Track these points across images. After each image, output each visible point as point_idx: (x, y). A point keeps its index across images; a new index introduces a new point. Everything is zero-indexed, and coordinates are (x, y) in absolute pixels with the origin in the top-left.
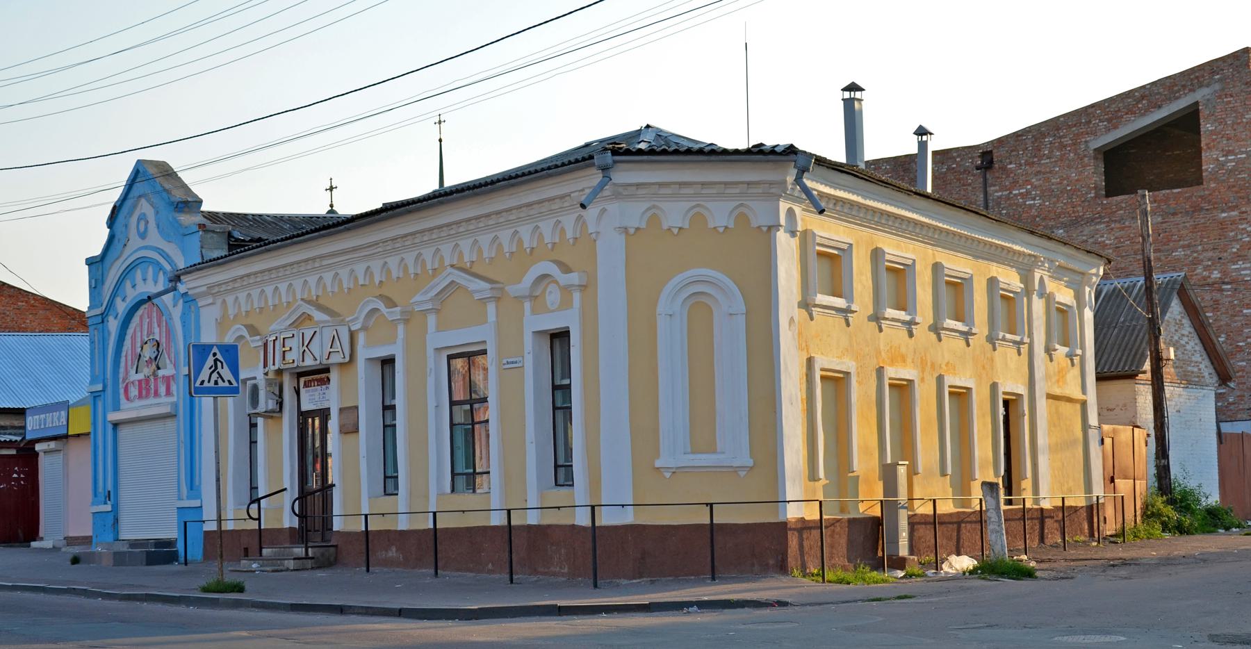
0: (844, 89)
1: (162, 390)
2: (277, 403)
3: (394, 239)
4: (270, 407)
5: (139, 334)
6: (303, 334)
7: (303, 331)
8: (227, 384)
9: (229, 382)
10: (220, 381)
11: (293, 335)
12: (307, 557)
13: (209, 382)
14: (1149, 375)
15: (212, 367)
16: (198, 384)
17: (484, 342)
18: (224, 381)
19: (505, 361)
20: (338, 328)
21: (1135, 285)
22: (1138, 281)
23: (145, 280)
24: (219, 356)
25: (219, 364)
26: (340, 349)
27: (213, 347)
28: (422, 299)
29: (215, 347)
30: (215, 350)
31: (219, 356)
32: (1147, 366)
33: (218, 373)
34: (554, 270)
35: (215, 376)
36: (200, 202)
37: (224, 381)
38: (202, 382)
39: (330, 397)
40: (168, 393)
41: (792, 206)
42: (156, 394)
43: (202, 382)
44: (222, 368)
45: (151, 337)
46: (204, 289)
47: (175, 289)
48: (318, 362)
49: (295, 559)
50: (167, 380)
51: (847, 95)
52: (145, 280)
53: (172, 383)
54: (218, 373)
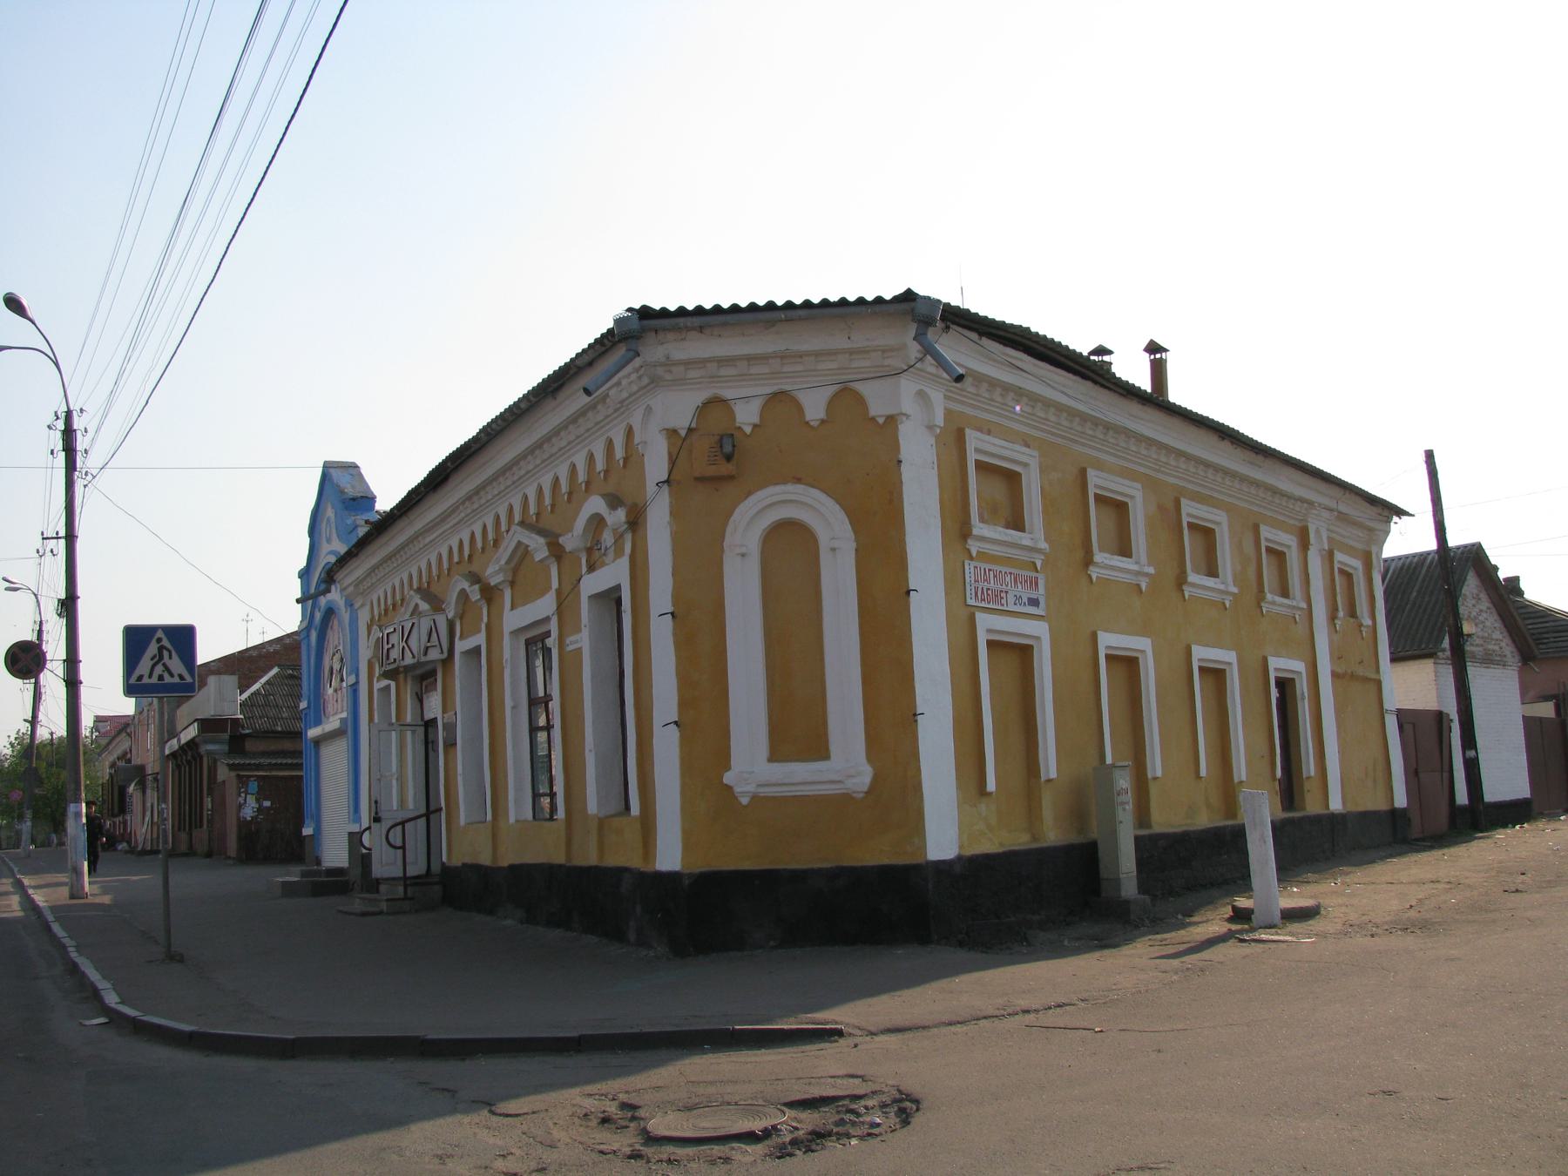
7: (402, 624)
8: (176, 680)
9: (181, 677)
10: (166, 675)
11: (395, 629)
12: (405, 898)
13: (150, 676)
14: (1448, 653)
15: (155, 656)
16: (133, 680)
18: (172, 675)
20: (434, 617)
25: (165, 653)
26: (437, 643)
31: (166, 642)
32: (1446, 643)
33: (164, 665)
35: (159, 669)
37: (172, 675)
38: (140, 678)
41: (922, 387)
43: (140, 678)
44: (170, 658)
48: (416, 660)
49: (388, 900)
54: (164, 665)
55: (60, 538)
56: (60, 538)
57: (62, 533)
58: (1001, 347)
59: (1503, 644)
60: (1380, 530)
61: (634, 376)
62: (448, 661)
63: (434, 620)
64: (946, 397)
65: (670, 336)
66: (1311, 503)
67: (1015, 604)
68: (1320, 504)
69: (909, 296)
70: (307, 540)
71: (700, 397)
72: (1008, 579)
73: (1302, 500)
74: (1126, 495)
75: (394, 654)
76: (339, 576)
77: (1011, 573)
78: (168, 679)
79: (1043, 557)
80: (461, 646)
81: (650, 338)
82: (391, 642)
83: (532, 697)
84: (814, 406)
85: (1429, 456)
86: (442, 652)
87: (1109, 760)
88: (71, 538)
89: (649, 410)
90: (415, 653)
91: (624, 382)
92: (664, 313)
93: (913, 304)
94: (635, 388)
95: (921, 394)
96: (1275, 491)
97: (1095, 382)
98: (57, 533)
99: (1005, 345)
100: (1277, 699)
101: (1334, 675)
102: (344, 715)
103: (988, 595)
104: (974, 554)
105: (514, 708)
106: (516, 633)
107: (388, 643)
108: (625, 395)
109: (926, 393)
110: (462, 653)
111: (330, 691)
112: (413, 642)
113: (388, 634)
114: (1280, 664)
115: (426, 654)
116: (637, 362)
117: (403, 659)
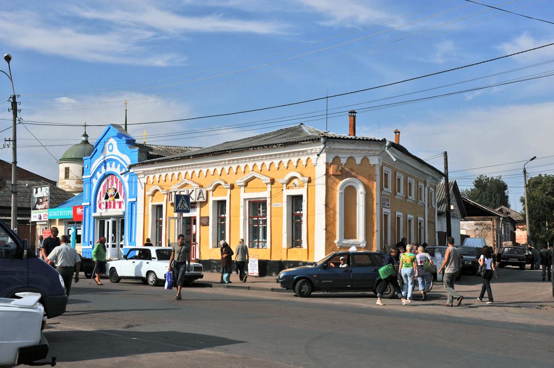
1: (117, 206)
3: (229, 161)
5: (106, 186)
8: (186, 209)
17: (266, 198)
19: (274, 204)
23: (111, 167)
28: (239, 181)
30: (183, 197)
34: (298, 175)
35: (182, 206)
36: (135, 141)
39: (195, 213)
40: (120, 207)
42: (114, 207)
45: (112, 187)
46: (141, 172)
47: (129, 171)
50: (120, 203)
52: (111, 167)
53: (122, 204)
62: (205, 203)
65: (331, 143)
71: (334, 156)
73: (428, 175)
78: (184, 209)
84: (358, 161)
85: (446, 153)
88: (15, 141)
96: (423, 173)
101: (428, 222)
115: (198, 199)
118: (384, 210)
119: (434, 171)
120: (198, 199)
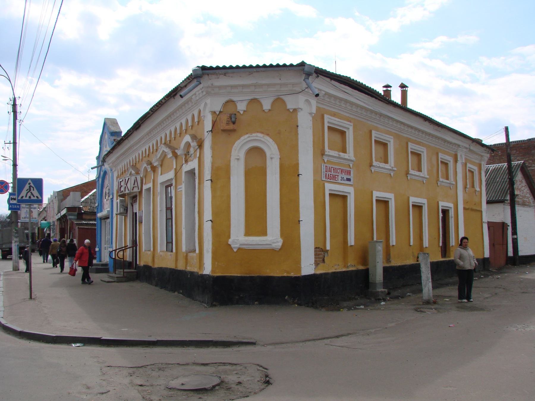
0: (384, 87)
2: (124, 210)
4: (121, 211)
6: (125, 179)
7: (125, 178)
8: (36, 198)
9: (37, 197)
11: (123, 180)
13: (26, 196)
14: (509, 201)
15: (28, 189)
18: (34, 196)
21: (503, 166)
22: (505, 165)
24: (32, 185)
25: (32, 188)
26: (137, 186)
27: (28, 181)
29: (30, 180)
31: (32, 185)
32: (508, 198)
33: (31, 193)
35: (29, 194)
37: (34, 196)
38: (22, 197)
41: (308, 99)
43: (22, 197)
44: (34, 190)
51: (385, 89)
54: (31, 193)
55: (11, 143)
56: (11, 143)
57: (12, 142)
58: (339, 84)
59: (530, 199)
60: (485, 156)
61: (200, 91)
62: (140, 192)
63: (136, 177)
64: (317, 102)
65: (214, 76)
66: (459, 146)
67: (341, 180)
68: (462, 146)
69: (302, 64)
70: (99, 146)
71: (224, 100)
72: (339, 171)
73: (455, 144)
74: (387, 141)
75: (122, 189)
76: (107, 160)
77: (340, 169)
78: (32, 198)
79: (353, 163)
80: (145, 187)
81: (206, 77)
82: (121, 185)
83: (167, 207)
84: (267, 105)
85: (507, 129)
86: (139, 189)
87: (375, 239)
88: (15, 143)
89: (206, 104)
90: (129, 190)
91: (197, 93)
92: (211, 68)
93: (303, 67)
94: (201, 96)
95: (307, 101)
96: (445, 141)
97: (376, 98)
98: (10, 142)
99: (341, 83)
100: (442, 217)
101: (465, 209)
102: (109, 209)
103: (330, 176)
104: (326, 161)
105: (160, 211)
106: (162, 184)
107: (120, 185)
108: (198, 98)
109: (309, 101)
110: (145, 189)
111: (105, 200)
112: (129, 185)
113: (120, 182)
114: (443, 204)
115: (133, 190)
116: (201, 86)
117: (125, 191)
118: (329, 187)
119: (421, 120)
120: (133, 190)
